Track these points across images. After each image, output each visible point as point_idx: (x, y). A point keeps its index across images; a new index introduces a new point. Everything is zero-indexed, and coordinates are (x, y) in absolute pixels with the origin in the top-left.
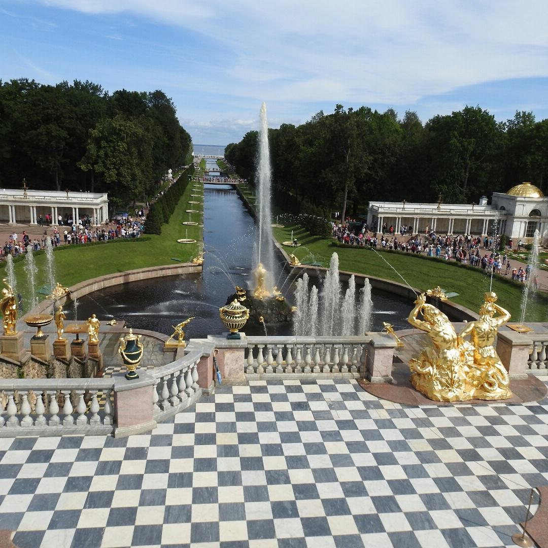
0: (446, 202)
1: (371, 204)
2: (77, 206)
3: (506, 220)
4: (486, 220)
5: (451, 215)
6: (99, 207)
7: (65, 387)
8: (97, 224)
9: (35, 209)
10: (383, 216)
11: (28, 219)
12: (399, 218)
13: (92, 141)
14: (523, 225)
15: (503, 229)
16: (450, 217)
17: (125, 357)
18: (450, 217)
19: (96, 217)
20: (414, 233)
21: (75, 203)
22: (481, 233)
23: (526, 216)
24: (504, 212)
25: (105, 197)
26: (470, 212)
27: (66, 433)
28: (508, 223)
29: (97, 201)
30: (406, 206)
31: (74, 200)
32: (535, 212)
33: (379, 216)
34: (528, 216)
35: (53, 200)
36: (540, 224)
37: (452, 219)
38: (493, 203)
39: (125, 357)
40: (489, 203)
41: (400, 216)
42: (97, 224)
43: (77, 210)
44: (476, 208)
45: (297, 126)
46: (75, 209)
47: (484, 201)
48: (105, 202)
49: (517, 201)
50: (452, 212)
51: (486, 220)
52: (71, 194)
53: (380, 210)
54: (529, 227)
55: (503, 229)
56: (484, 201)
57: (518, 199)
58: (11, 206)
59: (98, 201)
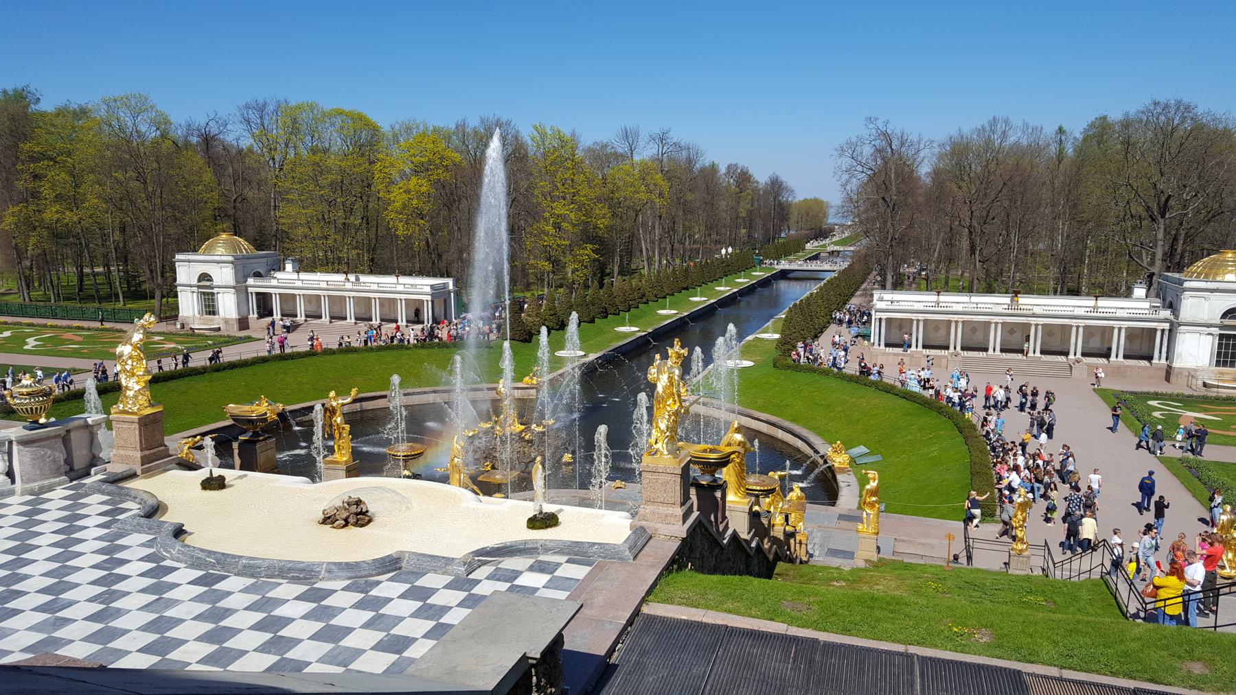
2: (403, 296)
5: (1034, 316)
6: (429, 298)
10: (884, 316)
12: (918, 321)
16: (1033, 321)
18: (1033, 321)
30: (942, 298)
35: (375, 287)
37: (1037, 325)
49: (1185, 290)
50: (1037, 310)
52: (404, 280)
55: (1164, 349)
56: (1139, 292)
57: (1187, 285)
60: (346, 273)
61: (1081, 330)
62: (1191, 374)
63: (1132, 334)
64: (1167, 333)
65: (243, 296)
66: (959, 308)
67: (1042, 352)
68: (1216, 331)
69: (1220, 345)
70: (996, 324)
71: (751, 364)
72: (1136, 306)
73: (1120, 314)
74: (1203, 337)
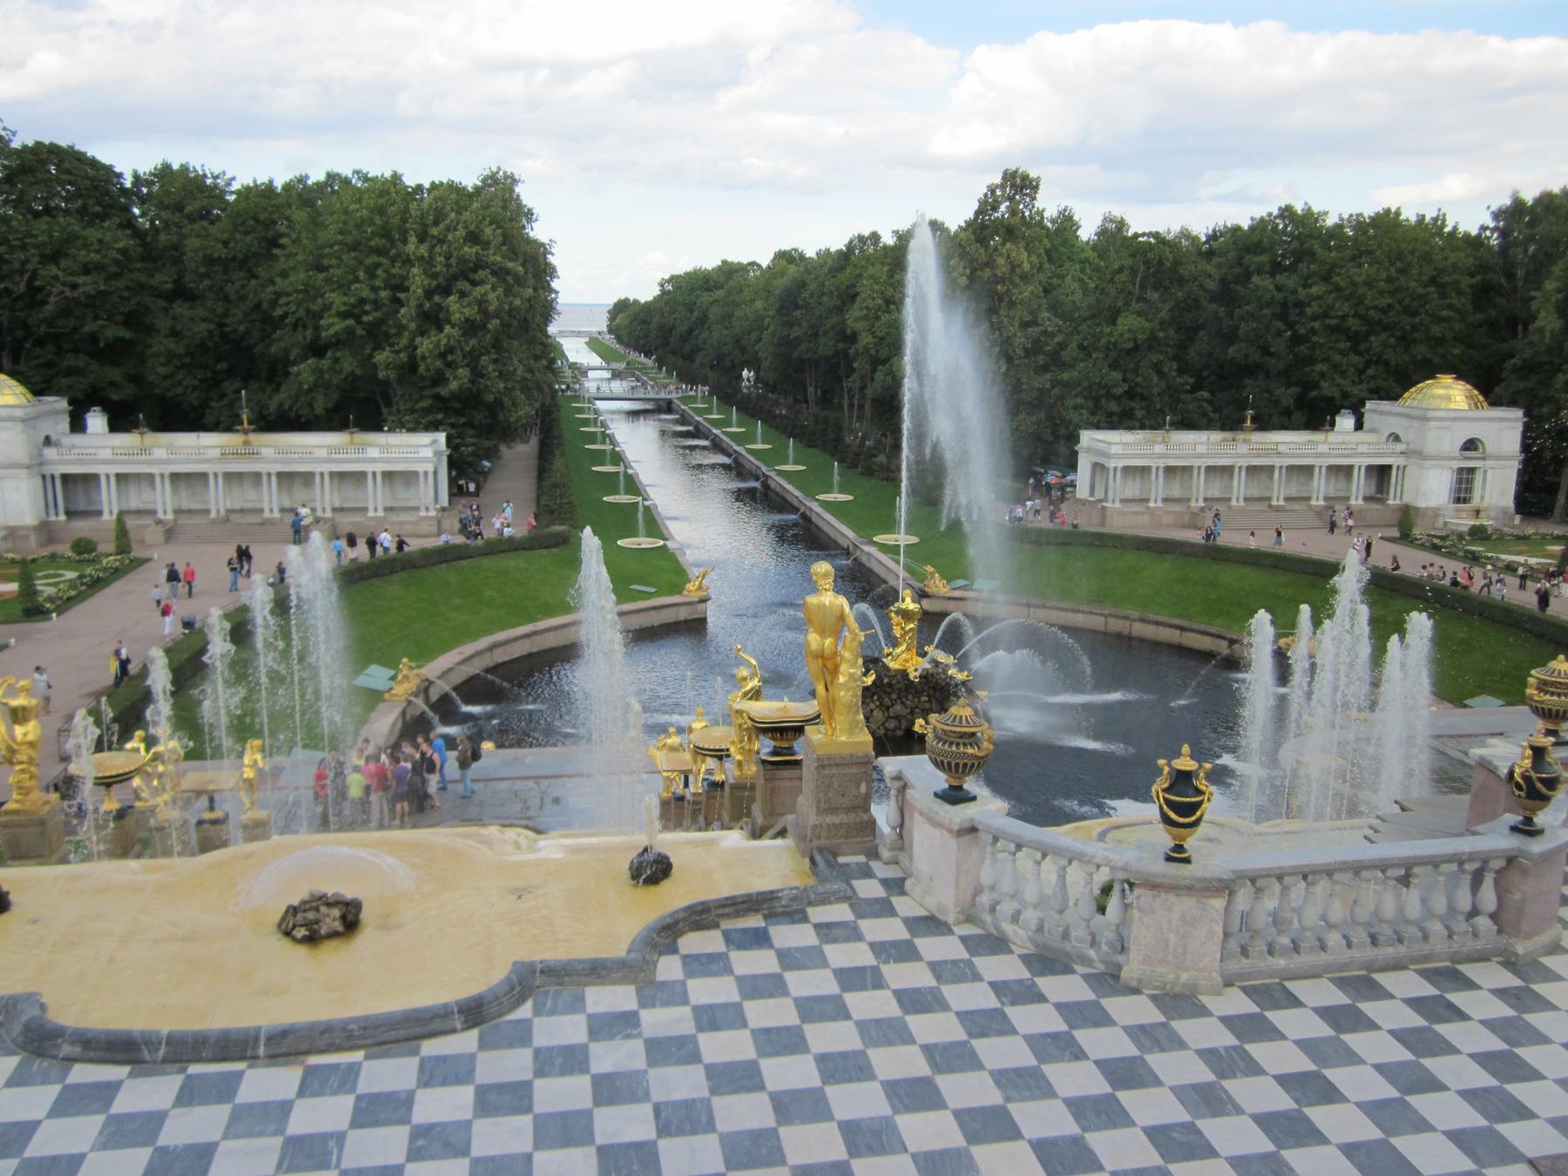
0: (1262, 425)
1: (1088, 437)
2: (380, 468)
6: (430, 468)
7: (1422, 857)
9: (274, 479)
10: (1121, 464)
11: (258, 505)
17: (1539, 785)
18: (1278, 462)
20: (1193, 504)
21: (373, 460)
22: (1348, 499)
24: (1400, 447)
25: (441, 437)
26: (1323, 448)
27: (1415, 961)
29: (423, 450)
31: (374, 453)
32: (1471, 445)
33: (1112, 464)
34: (1457, 453)
35: (323, 453)
38: (1366, 426)
39: (1539, 785)
40: (1359, 426)
41: (1162, 463)
43: (379, 478)
44: (1332, 437)
45: (810, 253)
47: (1345, 422)
49: (1428, 419)
50: (1282, 448)
53: (1114, 450)
54: (1460, 481)
57: (1431, 414)
58: (216, 475)
60: (246, 432)
62: (1436, 512)
65: (39, 480)
66: (1201, 449)
67: (1286, 499)
68: (1456, 465)
72: (1344, 440)
73: (1363, 449)
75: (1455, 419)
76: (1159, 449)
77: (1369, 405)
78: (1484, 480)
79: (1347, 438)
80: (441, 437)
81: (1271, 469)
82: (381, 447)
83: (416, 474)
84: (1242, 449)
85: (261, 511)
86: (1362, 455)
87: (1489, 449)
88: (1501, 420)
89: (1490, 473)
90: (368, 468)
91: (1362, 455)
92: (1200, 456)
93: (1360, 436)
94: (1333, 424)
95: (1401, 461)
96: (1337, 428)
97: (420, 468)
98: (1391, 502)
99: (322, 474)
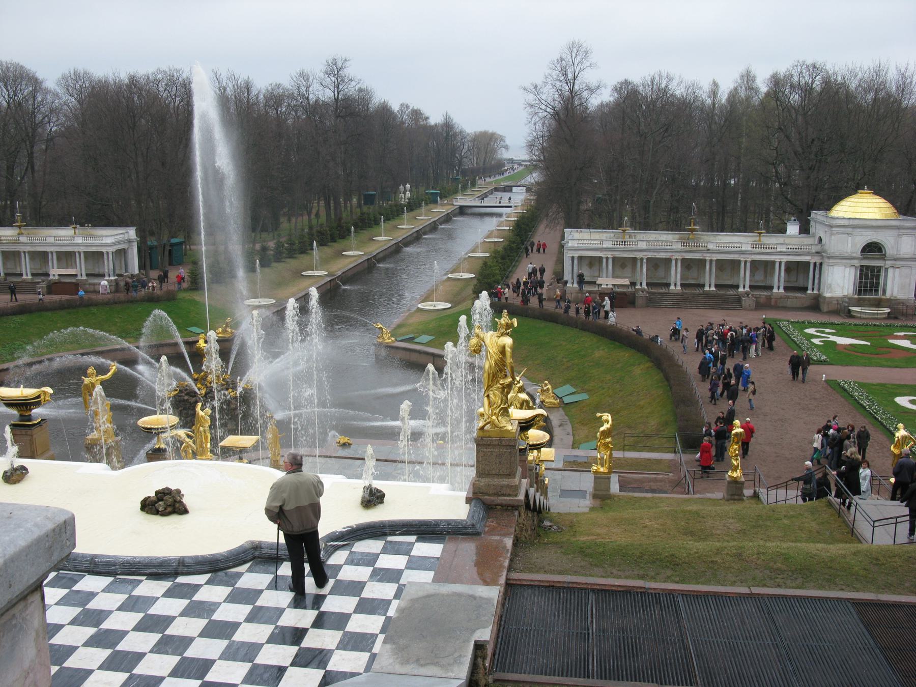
2: (82, 249)
3: (821, 264)
4: (780, 263)
8: (109, 276)
12: (607, 258)
13: (123, 145)
14: (853, 270)
15: (816, 281)
18: (708, 257)
19: (108, 265)
21: (78, 245)
23: (854, 255)
25: (132, 233)
26: (748, 248)
28: (825, 267)
31: (79, 240)
34: (859, 254)
35: (51, 240)
36: (886, 270)
38: (812, 230)
40: (805, 229)
41: (610, 255)
42: (109, 276)
44: (772, 240)
46: (79, 253)
47: (793, 229)
48: (130, 241)
50: (711, 246)
51: (780, 263)
56: (793, 229)
59: (109, 240)
60: (20, 227)
61: (748, 264)
63: (791, 267)
64: (818, 265)
67: (716, 286)
68: (857, 263)
69: (861, 275)
70: (676, 260)
71: (449, 305)
74: (847, 269)
75: (854, 227)
76: (607, 244)
77: (813, 215)
78: (886, 276)
79: (787, 241)
80: (132, 233)
81: (702, 262)
82: (85, 237)
83: (102, 253)
84: (679, 246)
85: (21, 275)
86: (781, 253)
87: (890, 250)
88: (898, 228)
89: (890, 271)
90: (76, 249)
91: (781, 253)
92: (641, 250)
93: (806, 240)
94: (784, 231)
95: (817, 259)
96: (788, 232)
97: (104, 250)
98: (809, 292)
99: (52, 253)
